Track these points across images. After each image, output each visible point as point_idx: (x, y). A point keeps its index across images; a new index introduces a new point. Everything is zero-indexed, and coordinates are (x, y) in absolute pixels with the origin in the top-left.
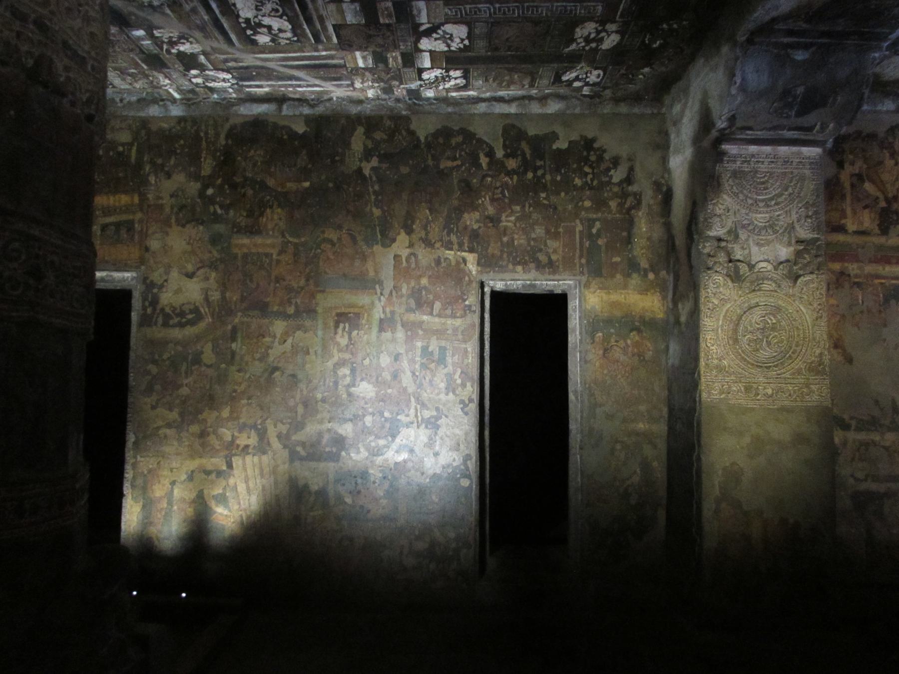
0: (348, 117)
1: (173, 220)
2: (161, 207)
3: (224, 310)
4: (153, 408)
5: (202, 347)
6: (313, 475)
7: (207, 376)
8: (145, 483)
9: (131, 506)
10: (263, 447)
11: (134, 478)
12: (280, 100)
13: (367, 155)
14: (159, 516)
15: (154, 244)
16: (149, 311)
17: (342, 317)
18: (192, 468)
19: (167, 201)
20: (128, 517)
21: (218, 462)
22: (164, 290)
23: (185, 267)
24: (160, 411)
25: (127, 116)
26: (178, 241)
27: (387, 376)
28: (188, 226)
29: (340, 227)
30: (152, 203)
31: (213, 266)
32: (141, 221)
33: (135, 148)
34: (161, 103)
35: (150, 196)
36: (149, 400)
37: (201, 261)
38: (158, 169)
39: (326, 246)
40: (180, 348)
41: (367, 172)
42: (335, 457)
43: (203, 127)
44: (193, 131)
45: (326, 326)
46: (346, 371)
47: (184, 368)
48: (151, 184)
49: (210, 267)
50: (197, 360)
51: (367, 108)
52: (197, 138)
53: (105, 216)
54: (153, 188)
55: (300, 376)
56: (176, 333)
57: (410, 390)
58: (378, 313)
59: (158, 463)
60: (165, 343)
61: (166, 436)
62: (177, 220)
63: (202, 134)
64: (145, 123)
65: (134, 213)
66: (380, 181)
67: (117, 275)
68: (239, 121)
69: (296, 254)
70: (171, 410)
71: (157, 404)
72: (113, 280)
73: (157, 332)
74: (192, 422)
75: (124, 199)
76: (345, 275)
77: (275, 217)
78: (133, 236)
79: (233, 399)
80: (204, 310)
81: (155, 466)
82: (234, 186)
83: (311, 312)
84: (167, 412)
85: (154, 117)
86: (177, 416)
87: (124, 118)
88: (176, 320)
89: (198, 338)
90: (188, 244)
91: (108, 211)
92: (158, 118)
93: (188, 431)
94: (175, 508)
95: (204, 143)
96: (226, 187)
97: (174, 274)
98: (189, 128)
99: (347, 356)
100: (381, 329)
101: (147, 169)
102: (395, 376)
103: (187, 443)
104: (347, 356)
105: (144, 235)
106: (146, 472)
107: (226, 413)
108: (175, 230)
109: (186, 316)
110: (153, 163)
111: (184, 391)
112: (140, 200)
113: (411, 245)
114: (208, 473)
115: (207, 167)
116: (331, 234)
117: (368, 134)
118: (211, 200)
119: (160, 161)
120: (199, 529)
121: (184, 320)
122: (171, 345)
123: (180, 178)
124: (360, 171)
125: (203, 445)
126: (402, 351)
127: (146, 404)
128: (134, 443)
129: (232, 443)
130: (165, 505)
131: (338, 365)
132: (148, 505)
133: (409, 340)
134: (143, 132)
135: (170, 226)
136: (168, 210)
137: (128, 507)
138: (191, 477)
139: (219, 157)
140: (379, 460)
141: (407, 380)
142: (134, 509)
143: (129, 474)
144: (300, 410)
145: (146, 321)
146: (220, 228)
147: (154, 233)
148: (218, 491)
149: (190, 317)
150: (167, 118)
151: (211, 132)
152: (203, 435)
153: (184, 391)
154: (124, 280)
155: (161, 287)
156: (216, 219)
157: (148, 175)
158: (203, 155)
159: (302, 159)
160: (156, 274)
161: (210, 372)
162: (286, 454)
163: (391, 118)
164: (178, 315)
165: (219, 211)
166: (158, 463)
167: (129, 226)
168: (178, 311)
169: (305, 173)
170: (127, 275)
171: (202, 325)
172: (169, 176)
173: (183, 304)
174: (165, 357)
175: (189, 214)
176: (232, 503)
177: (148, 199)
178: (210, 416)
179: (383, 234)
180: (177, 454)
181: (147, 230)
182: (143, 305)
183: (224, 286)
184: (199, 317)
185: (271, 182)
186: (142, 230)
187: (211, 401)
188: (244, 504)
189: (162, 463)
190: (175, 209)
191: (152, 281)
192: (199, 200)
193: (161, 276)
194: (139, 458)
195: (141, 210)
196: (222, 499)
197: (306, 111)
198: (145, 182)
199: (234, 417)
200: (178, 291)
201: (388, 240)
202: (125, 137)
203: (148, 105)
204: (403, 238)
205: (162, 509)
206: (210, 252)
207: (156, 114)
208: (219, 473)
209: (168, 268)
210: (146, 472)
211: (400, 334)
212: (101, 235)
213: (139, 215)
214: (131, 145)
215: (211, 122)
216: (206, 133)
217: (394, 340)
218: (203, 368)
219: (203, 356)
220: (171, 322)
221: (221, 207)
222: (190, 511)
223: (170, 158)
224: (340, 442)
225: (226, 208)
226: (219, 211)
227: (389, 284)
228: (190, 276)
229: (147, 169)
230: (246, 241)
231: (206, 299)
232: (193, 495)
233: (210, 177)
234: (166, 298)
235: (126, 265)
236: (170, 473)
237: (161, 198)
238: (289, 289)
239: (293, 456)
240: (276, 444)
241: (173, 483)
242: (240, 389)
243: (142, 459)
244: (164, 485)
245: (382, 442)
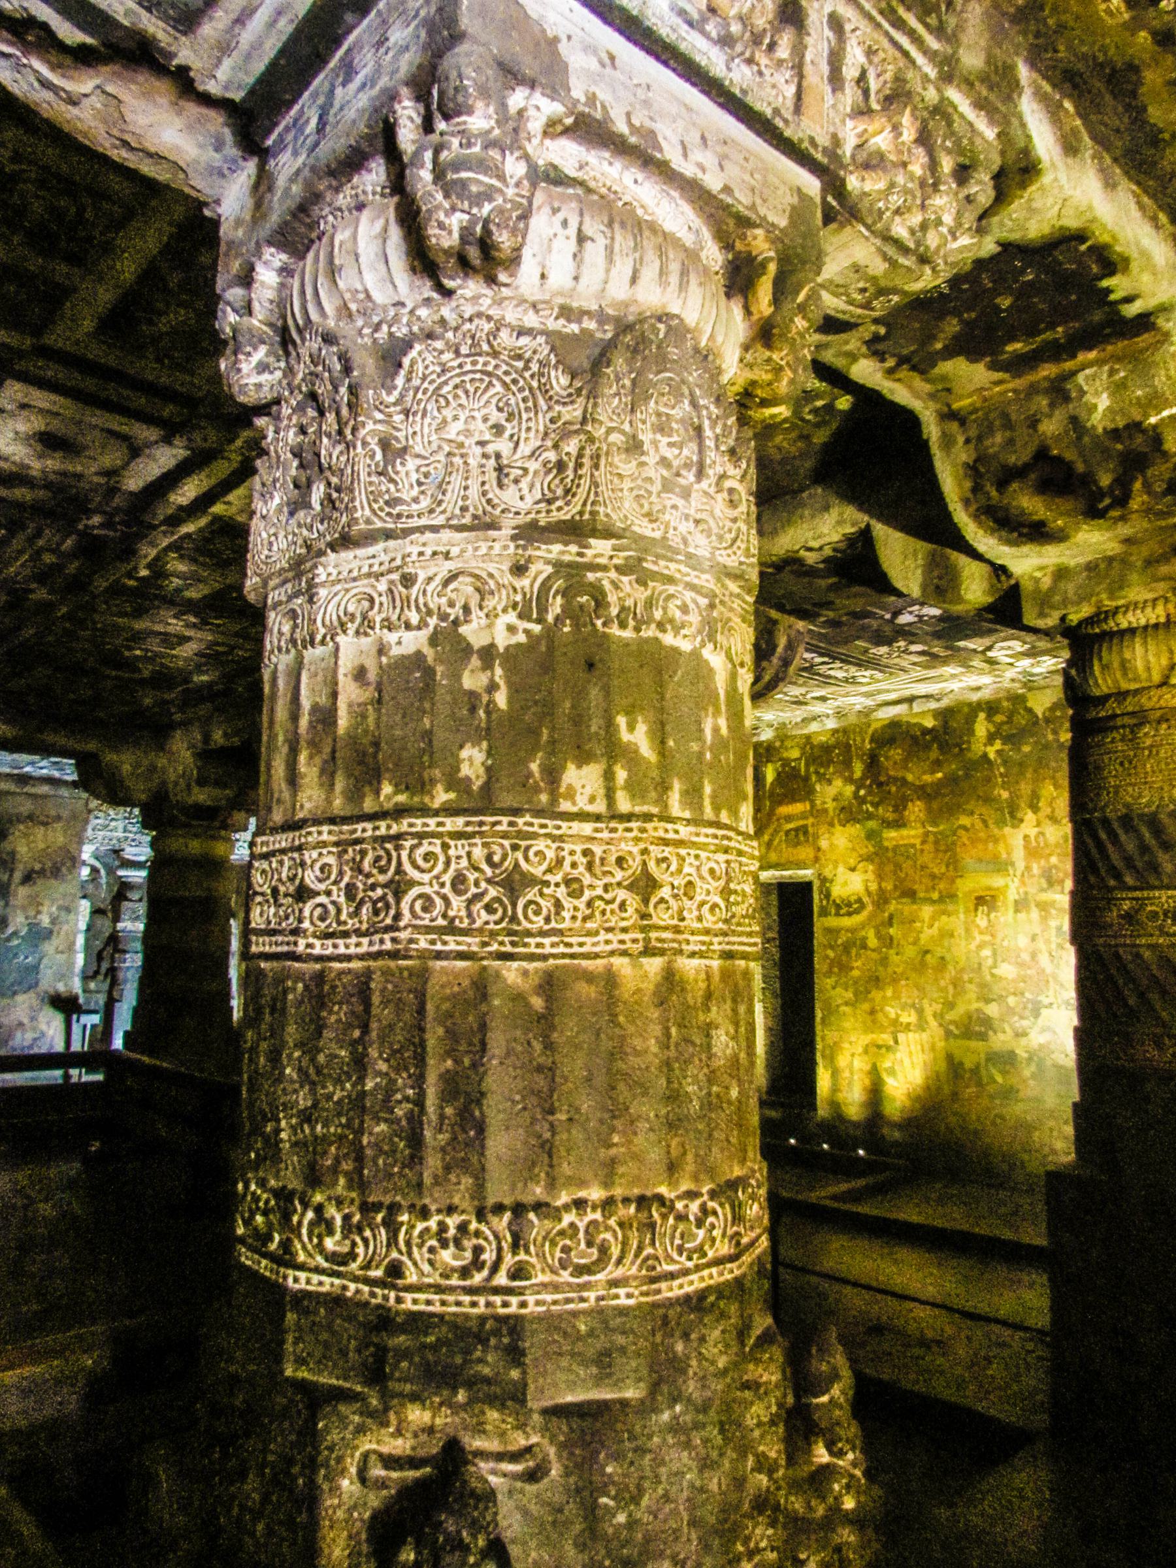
0: (970, 704)
2: (826, 811)
3: (882, 900)
6: (972, 1053)
10: (921, 1026)
12: (911, 700)
13: (991, 739)
15: (824, 843)
17: (980, 901)
19: (830, 805)
21: (886, 1038)
27: (1025, 957)
29: (972, 813)
31: (868, 859)
36: (830, 982)
38: (821, 777)
39: (961, 832)
41: (992, 756)
42: (983, 1037)
45: (967, 911)
46: (986, 952)
50: (864, 946)
51: (985, 694)
52: (848, 746)
55: (948, 957)
56: (847, 922)
57: (1048, 971)
58: (1012, 895)
64: (808, 737)
66: (1005, 763)
67: (801, 872)
68: (878, 725)
69: (936, 842)
73: (832, 921)
76: (980, 860)
77: (916, 809)
79: (895, 981)
80: (866, 899)
82: (880, 785)
83: (952, 896)
89: (863, 926)
91: (789, 818)
97: (841, 869)
99: (987, 938)
100: (1017, 911)
102: (1034, 955)
104: (987, 938)
105: (816, 837)
107: (889, 993)
108: (838, 828)
109: (850, 907)
113: (1038, 824)
114: (879, 1047)
115: (858, 769)
116: (965, 820)
117: (989, 718)
118: (863, 801)
124: (985, 755)
125: (874, 1021)
126: (1038, 931)
129: (895, 1022)
131: (980, 947)
132: (835, 1073)
133: (1044, 919)
138: (866, 1051)
140: (1023, 1041)
141: (1044, 960)
143: (819, 1046)
144: (951, 989)
145: (824, 912)
146: (872, 824)
148: (887, 1064)
152: (872, 1012)
156: (870, 816)
159: (934, 754)
161: (874, 955)
162: (941, 1032)
163: (1008, 699)
167: (804, 830)
169: (937, 765)
171: (865, 914)
172: (829, 782)
175: (849, 814)
176: (900, 1075)
178: (876, 995)
179: (1013, 816)
183: (880, 877)
184: (863, 906)
185: (910, 777)
187: (876, 981)
188: (910, 1078)
196: (892, 1072)
197: (933, 705)
199: (897, 996)
201: (1017, 821)
202: (795, 754)
204: (1030, 816)
208: (888, 1048)
211: (1035, 914)
217: (1030, 921)
222: (867, 1082)
224: (987, 1022)
225: (876, 805)
227: (1020, 865)
228: (853, 870)
230: (893, 834)
232: (868, 1067)
234: (837, 891)
238: (933, 877)
239: (948, 1034)
240: (933, 1023)
242: (899, 970)
245: (1025, 1023)
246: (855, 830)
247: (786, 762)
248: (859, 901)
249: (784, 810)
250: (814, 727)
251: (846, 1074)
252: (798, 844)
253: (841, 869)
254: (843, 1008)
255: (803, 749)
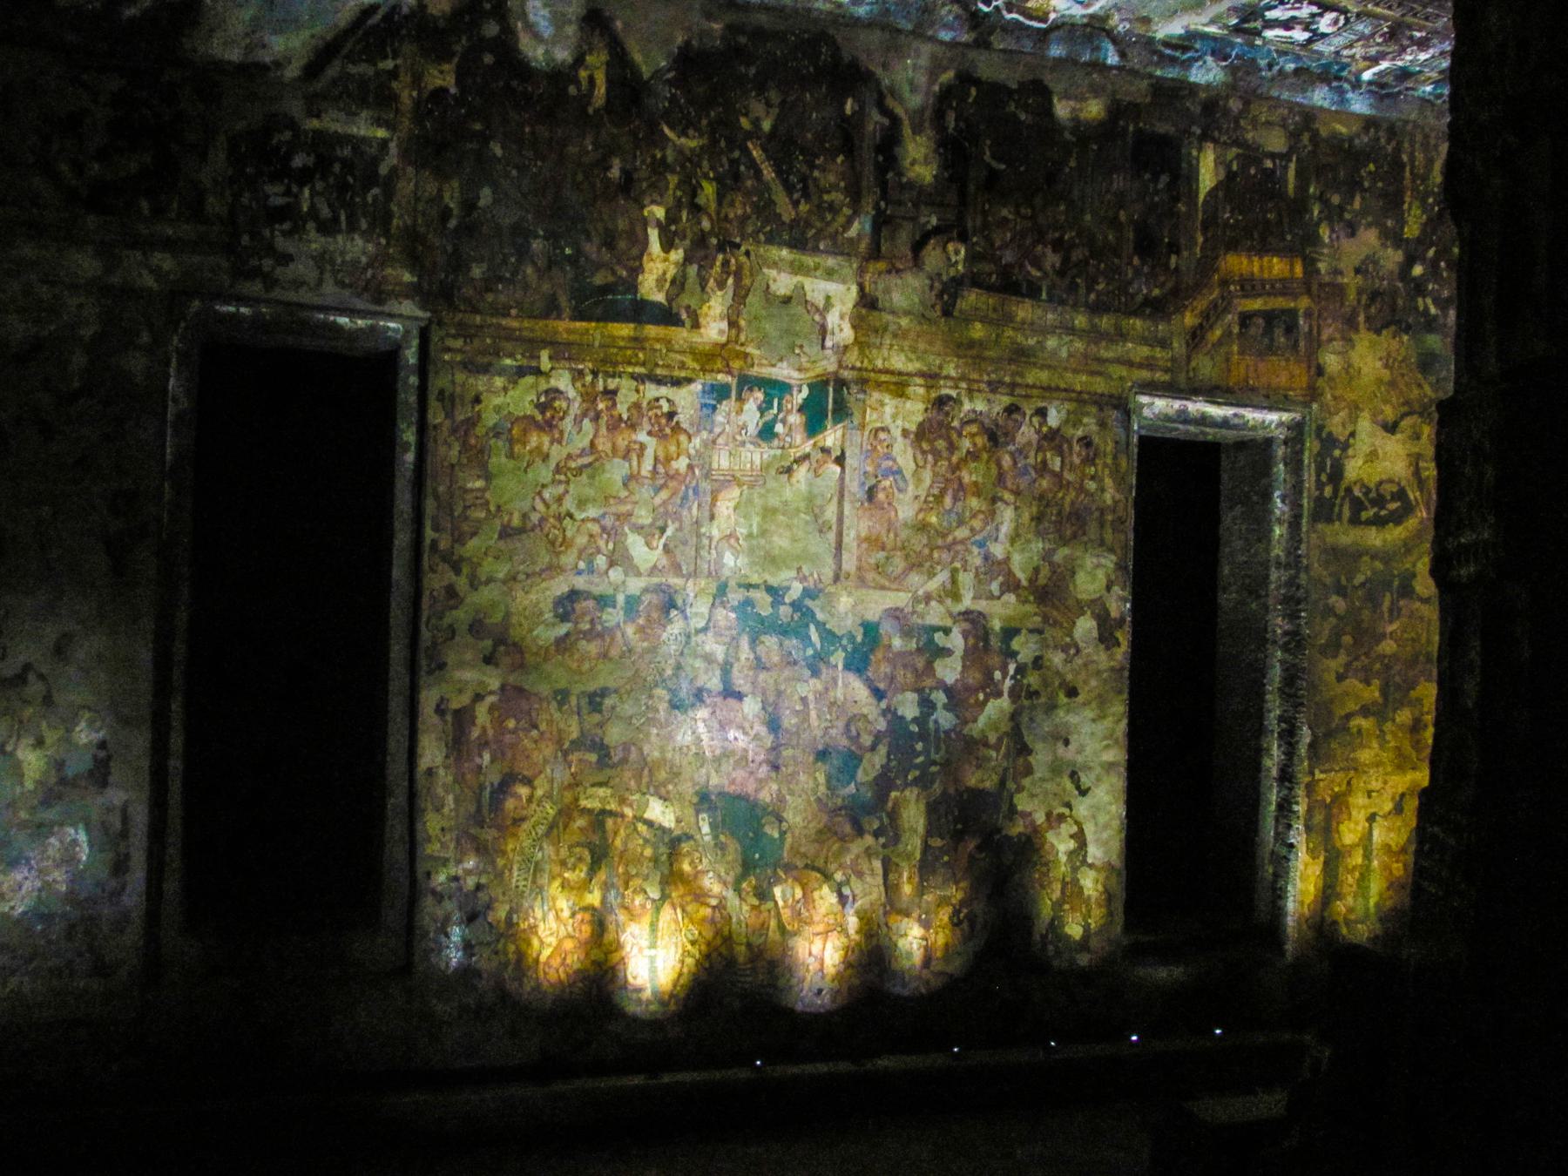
1: (1361, 318)
2: (1340, 290)
4: (1340, 678)
5: (1414, 565)
7: (1422, 618)
8: (1328, 819)
9: (1306, 865)
11: (1310, 811)
14: (1350, 880)
15: (1331, 361)
16: (1328, 491)
18: (1400, 790)
19: (1350, 280)
20: (1299, 885)
22: (1350, 452)
23: (1382, 412)
24: (1353, 683)
25: (1278, 98)
26: (1366, 358)
28: (1384, 332)
30: (1327, 279)
32: (1308, 314)
33: (1292, 166)
34: (1335, 84)
35: (1322, 266)
36: (1335, 664)
37: (1406, 403)
38: (1333, 215)
40: (1378, 565)
43: (1406, 145)
44: (1389, 149)
47: (1386, 604)
48: (1324, 245)
49: (1421, 415)
53: (1246, 296)
54: (1326, 251)
56: (1374, 538)
59: (1349, 783)
60: (1354, 555)
61: (1359, 731)
62: (1368, 319)
63: (1405, 158)
64: (1309, 116)
65: (1295, 297)
67: (1252, 415)
70: (1368, 683)
71: (1347, 670)
72: (1244, 426)
73: (1343, 535)
74: (1401, 704)
75: (1277, 266)
78: (1296, 341)
81: (1344, 787)
84: (1361, 686)
85: (1321, 108)
86: (1377, 694)
87: (1276, 103)
88: (1371, 512)
90: (1386, 366)
91: (1250, 286)
92: (1329, 111)
93: (1394, 720)
94: (1375, 863)
95: (1407, 174)
96: (1443, 264)
97: (1365, 425)
98: (1383, 141)
101: (1316, 213)
103: (1392, 744)
105: (1315, 343)
106: (1328, 800)
110: (1322, 199)
111: (1388, 647)
112: (1305, 273)
118: (1419, 288)
119: (1336, 199)
120: (1086, 928)
121: (1383, 513)
122: (1366, 558)
123: (1369, 237)
127: (1328, 669)
128: (1311, 746)
130: (1359, 860)
132: (1333, 861)
134: (1306, 137)
135: (1357, 330)
136: (1352, 296)
137: (1301, 867)
139: (1432, 206)
142: (1309, 872)
147: (1331, 340)
149: (1394, 506)
150: (1344, 115)
151: (1419, 156)
153: (1388, 647)
154: (1263, 425)
155: (1345, 446)
157: (1318, 225)
158: (1407, 199)
160: (1337, 419)
164: (1374, 503)
165: (1433, 310)
166: (1349, 783)
167: (1289, 321)
168: (1373, 495)
170: (1273, 417)
171: (1412, 523)
172: (1352, 229)
173: (1381, 483)
174: (1360, 579)
177: (1318, 271)
180: (1378, 764)
181: (1319, 334)
182: (1318, 480)
184: (1407, 509)
186: (1311, 330)
189: (1354, 781)
190: (1364, 298)
191: (1330, 434)
192: (1400, 285)
193: (1344, 425)
194: (1318, 775)
195: (1309, 292)
198: (1312, 239)
200: (1373, 456)
202: (1276, 142)
203: (1313, 83)
205: (1354, 868)
206: (1420, 386)
207: (1326, 104)
209: (1355, 409)
210: (1328, 800)
212: (1241, 334)
213: (1304, 303)
214: (1286, 157)
215: (1419, 138)
216: (1412, 158)
218: (1418, 604)
219: (1414, 583)
220: (1364, 515)
221: (1436, 302)
223: (1353, 197)
226: (1433, 310)
228: (1391, 428)
229: (1316, 213)
231: (1417, 472)
233: (1419, 241)
234: (1354, 469)
235: (1286, 397)
236: (1367, 801)
237: (1341, 273)
241: (1372, 818)
243: (1322, 776)
244: (1357, 823)
246: (1398, 344)
247: (1252, 155)
248: (1401, 495)
249: (1237, 263)
250: (1320, 97)
251: (1357, 859)
252: (1271, 349)
253: (1365, 425)
254: (1359, 722)
255: (1294, 136)
